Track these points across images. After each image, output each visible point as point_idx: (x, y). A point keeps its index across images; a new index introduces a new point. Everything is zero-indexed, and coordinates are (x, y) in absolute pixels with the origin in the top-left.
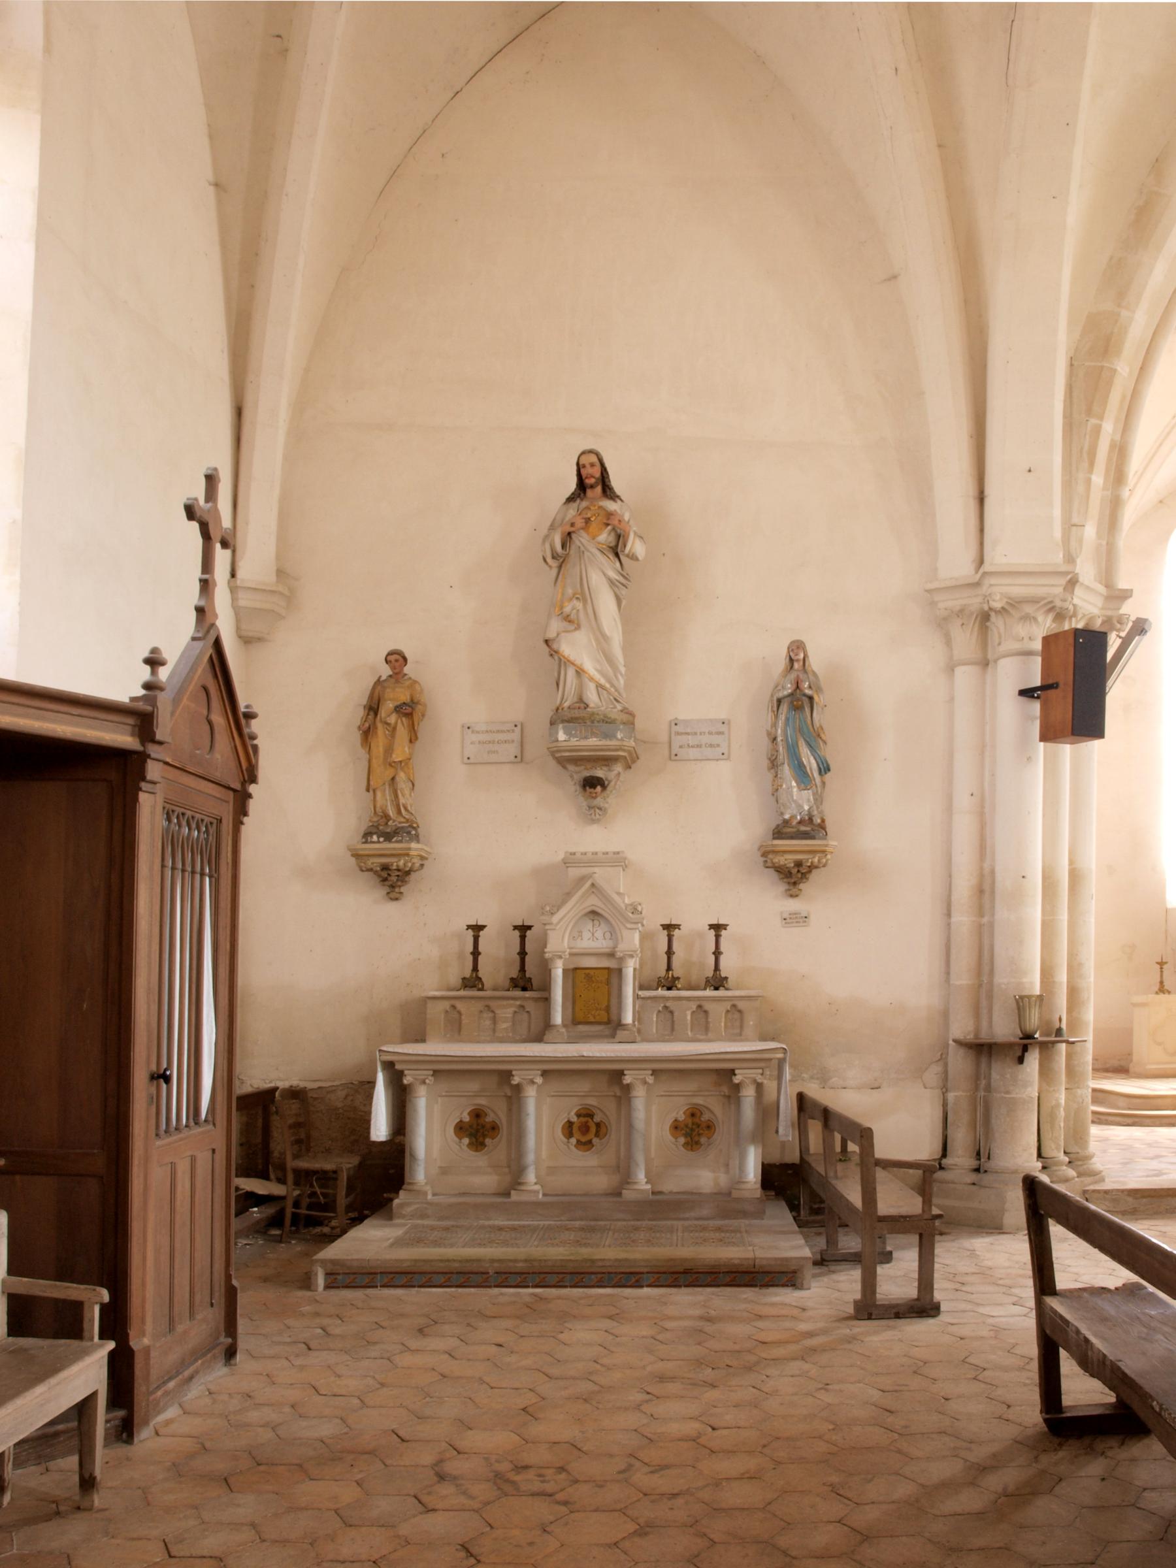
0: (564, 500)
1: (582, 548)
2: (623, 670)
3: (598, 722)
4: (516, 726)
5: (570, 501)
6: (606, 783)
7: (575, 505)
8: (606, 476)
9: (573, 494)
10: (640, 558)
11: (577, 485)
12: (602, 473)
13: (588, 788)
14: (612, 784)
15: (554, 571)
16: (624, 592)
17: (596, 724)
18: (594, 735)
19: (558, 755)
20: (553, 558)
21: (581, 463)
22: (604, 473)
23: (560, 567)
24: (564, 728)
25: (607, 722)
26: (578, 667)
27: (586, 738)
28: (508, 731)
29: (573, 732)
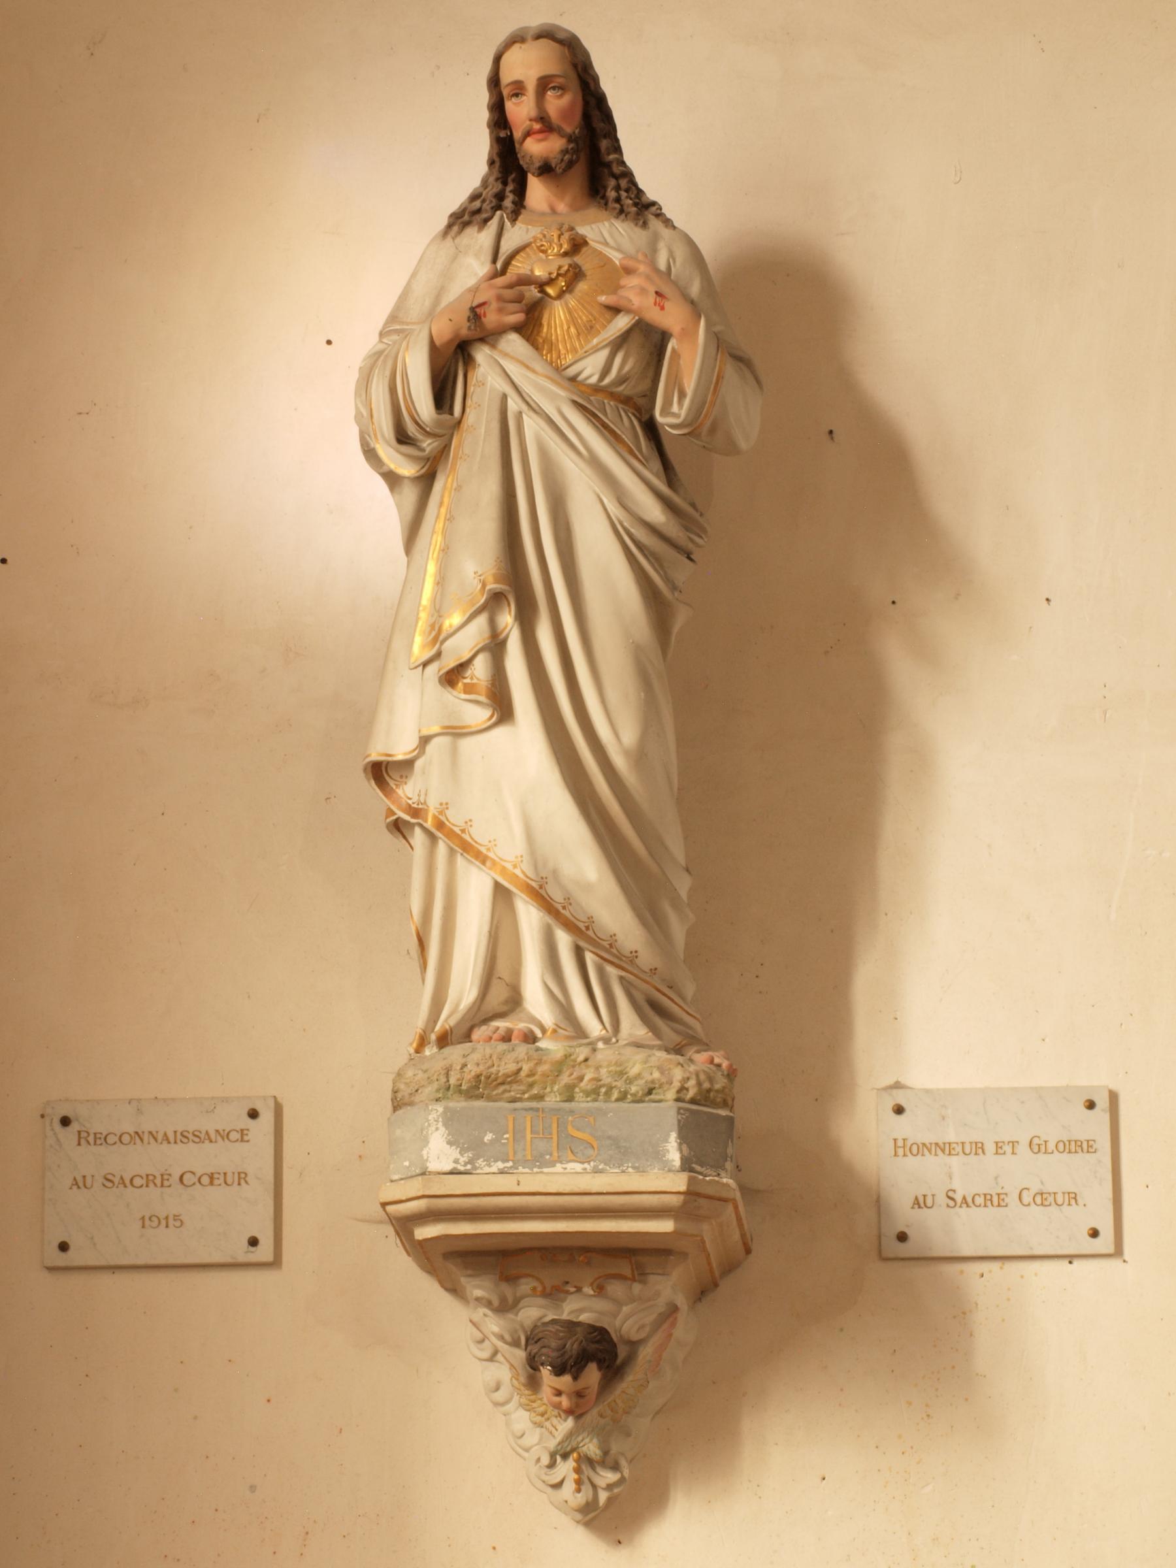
0: (444, 222)
1: (514, 404)
2: (683, 885)
3: (594, 1093)
4: (253, 1114)
5: (466, 224)
6: (622, 1352)
7: (483, 238)
8: (599, 125)
9: (474, 197)
10: (743, 445)
11: (491, 163)
12: (586, 117)
13: (546, 1372)
14: (646, 1353)
15: (410, 494)
16: (683, 572)
17: (582, 1103)
18: (569, 1147)
19: (425, 1232)
20: (402, 438)
21: (506, 77)
22: (595, 113)
23: (427, 480)
24: (449, 1119)
25: (622, 1098)
26: (504, 871)
27: (539, 1161)
28: (225, 1136)
29: (489, 1137)
